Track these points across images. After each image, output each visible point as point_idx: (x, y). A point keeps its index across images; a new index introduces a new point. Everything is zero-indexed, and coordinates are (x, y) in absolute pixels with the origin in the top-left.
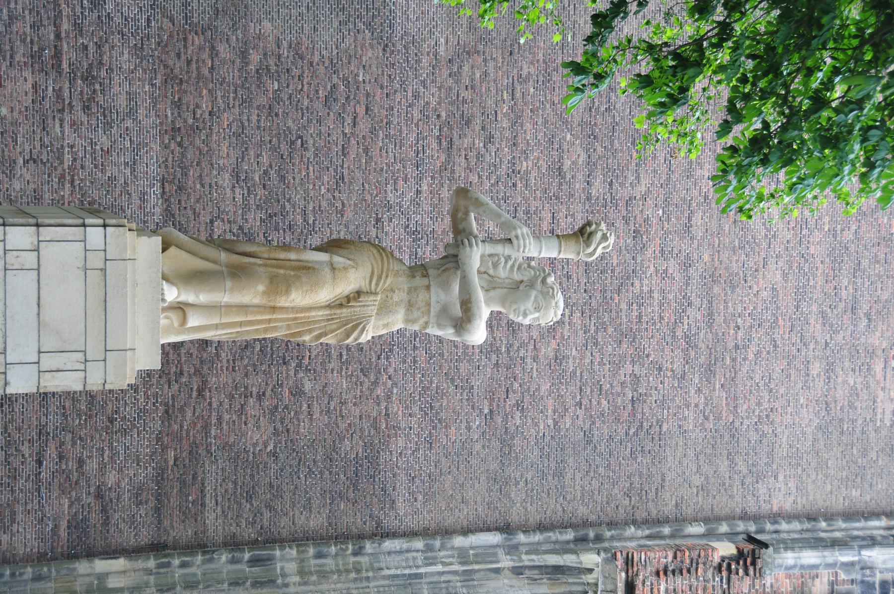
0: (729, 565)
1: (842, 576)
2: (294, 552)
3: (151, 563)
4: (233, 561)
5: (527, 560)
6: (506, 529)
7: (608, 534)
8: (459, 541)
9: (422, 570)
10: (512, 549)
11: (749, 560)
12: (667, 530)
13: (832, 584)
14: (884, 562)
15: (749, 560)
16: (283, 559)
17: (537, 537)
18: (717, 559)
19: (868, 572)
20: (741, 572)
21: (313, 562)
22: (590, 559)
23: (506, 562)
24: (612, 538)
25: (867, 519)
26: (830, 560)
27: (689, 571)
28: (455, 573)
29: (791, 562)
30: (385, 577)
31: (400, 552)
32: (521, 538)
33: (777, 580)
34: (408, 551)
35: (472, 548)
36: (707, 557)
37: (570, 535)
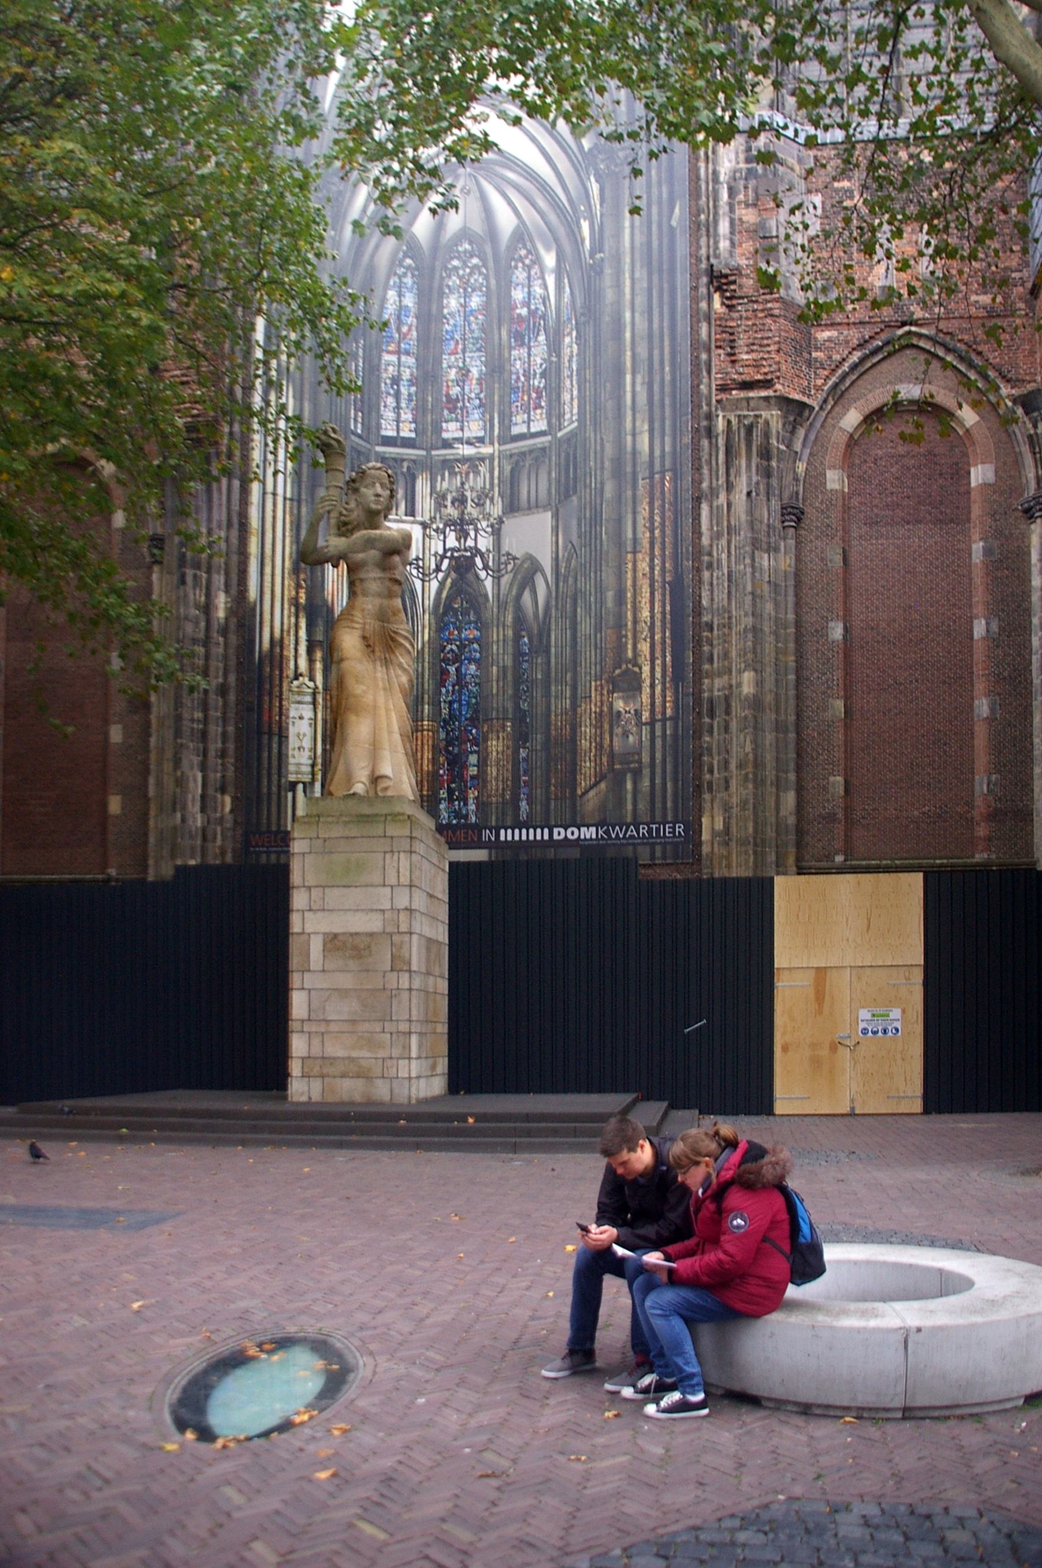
0: (728, 298)
1: (741, 197)
2: (706, 681)
3: (707, 796)
4: (711, 732)
5: (722, 480)
6: (697, 500)
7: (705, 408)
8: (705, 541)
9: (726, 571)
10: (714, 492)
11: (724, 281)
12: (704, 356)
13: (747, 206)
14: (730, 161)
15: (724, 281)
16: (711, 690)
17: (705, 471)
18: (724, 310)
19: (738, 175)
20: (732, 287)
21: (715, 665)
22: (720, 424)
23: (722, 499)
24: (709, 404)
25: (698, 178)
26: (727, 209)
27: (732, 334)
28: (729, 542)
29: (727, 243)
30: (729, 603)
31: (712, 591)
32: (705, 485)
33: (743, 254)
34: (711, 584)
35: (712, 529)
36: (720, 319)
37: (705, 443)
